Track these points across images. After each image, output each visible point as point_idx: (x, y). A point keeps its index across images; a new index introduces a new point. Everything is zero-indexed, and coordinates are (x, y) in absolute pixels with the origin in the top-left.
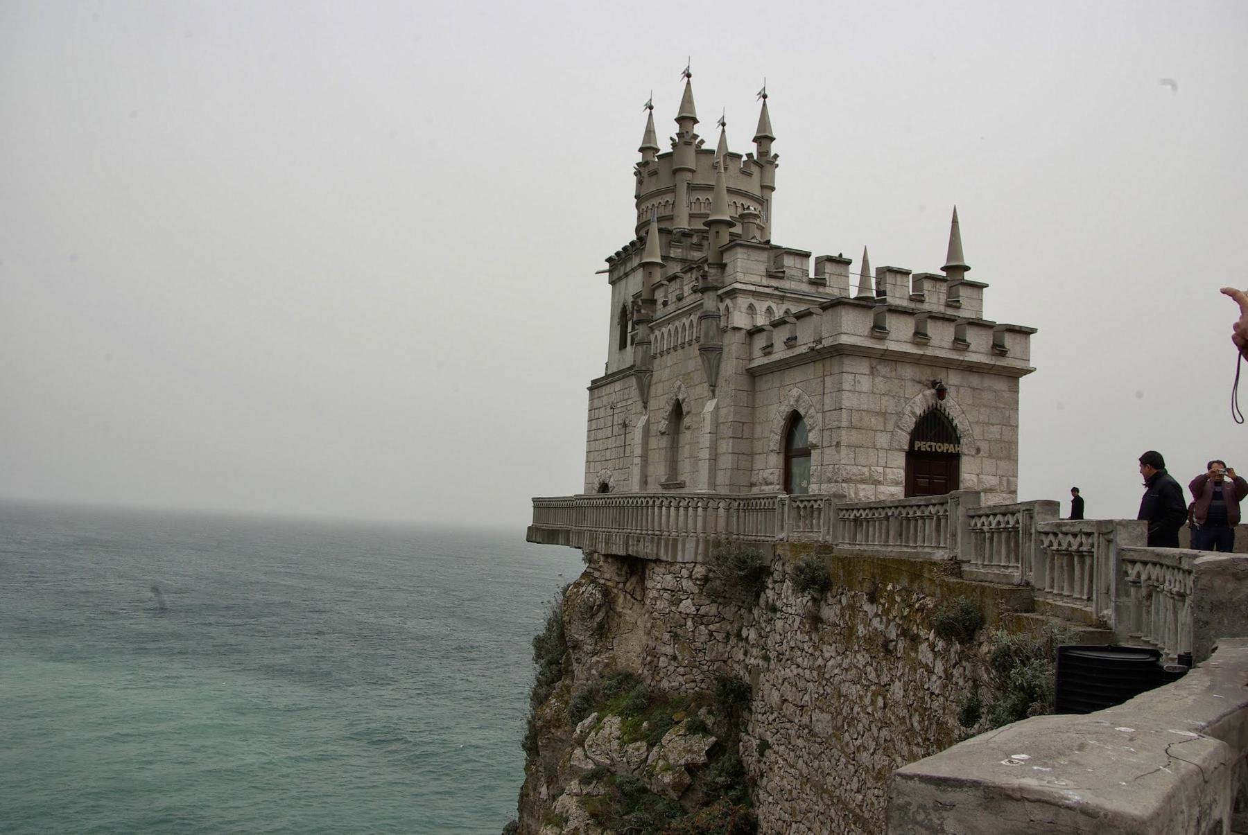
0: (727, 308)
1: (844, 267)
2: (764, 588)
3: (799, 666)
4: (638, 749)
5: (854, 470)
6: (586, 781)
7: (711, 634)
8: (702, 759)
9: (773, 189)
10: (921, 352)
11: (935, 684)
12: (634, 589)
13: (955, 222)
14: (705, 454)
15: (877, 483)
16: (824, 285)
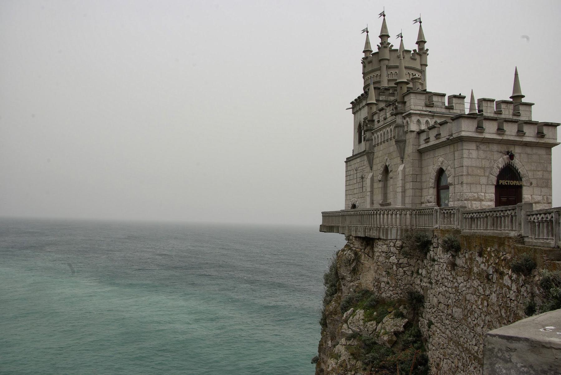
0: (407, 122)
1: (462, 99)
2: (429, 250)
3: (446, 287)
4: (372, 325)
5: (470, 195)
6: (349, 338)
7: (405, 272)
8: (401, 329)
9: (426, 65)
10: (501, 138)
11: (512, 295)
12: (369, 252)
13: (516, 74)
14: (399, 190)
15: (481, 200)
16: (453, 109)
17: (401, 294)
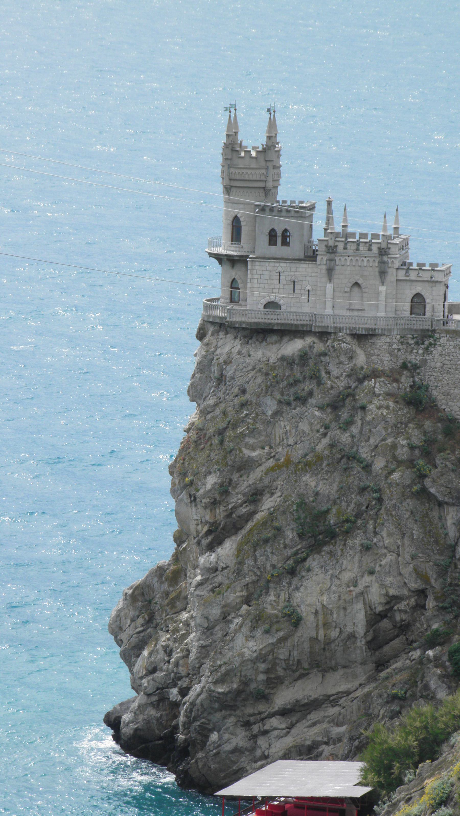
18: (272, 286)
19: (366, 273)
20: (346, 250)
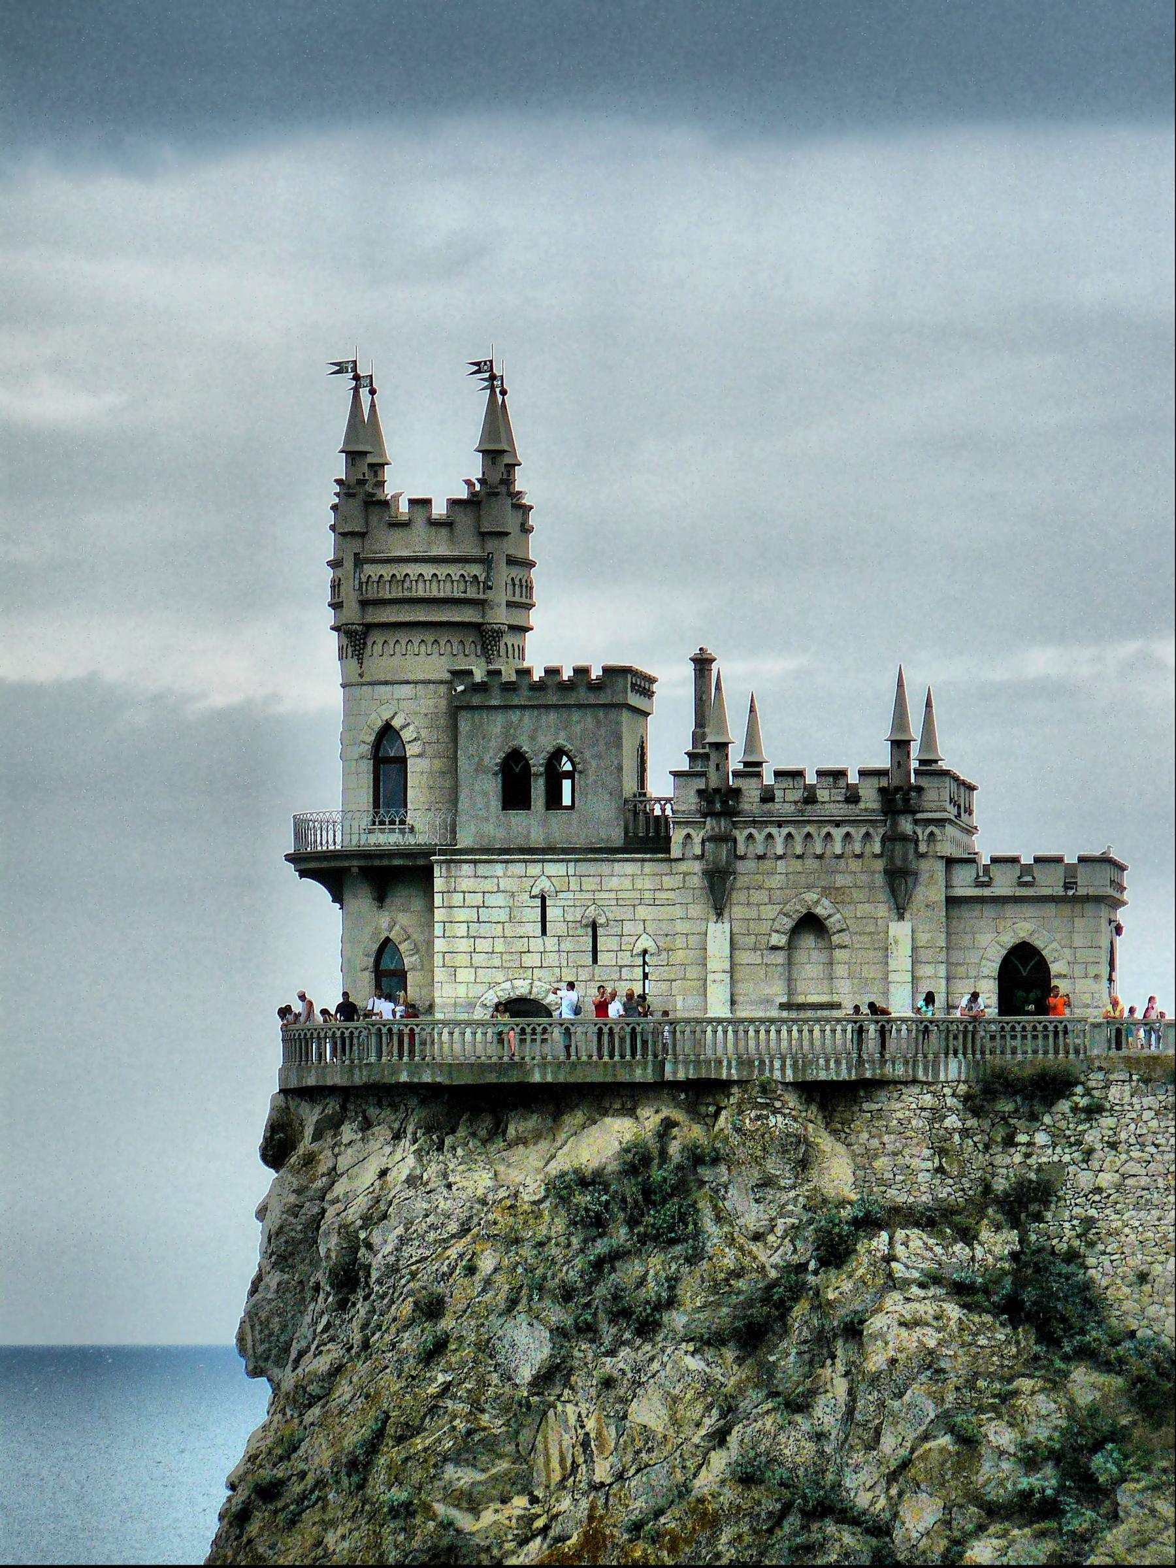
3: (1157, 1146)
17: (970, 1188)
18: (520, 945)
19: (840, 880)
20: (769, 806)
